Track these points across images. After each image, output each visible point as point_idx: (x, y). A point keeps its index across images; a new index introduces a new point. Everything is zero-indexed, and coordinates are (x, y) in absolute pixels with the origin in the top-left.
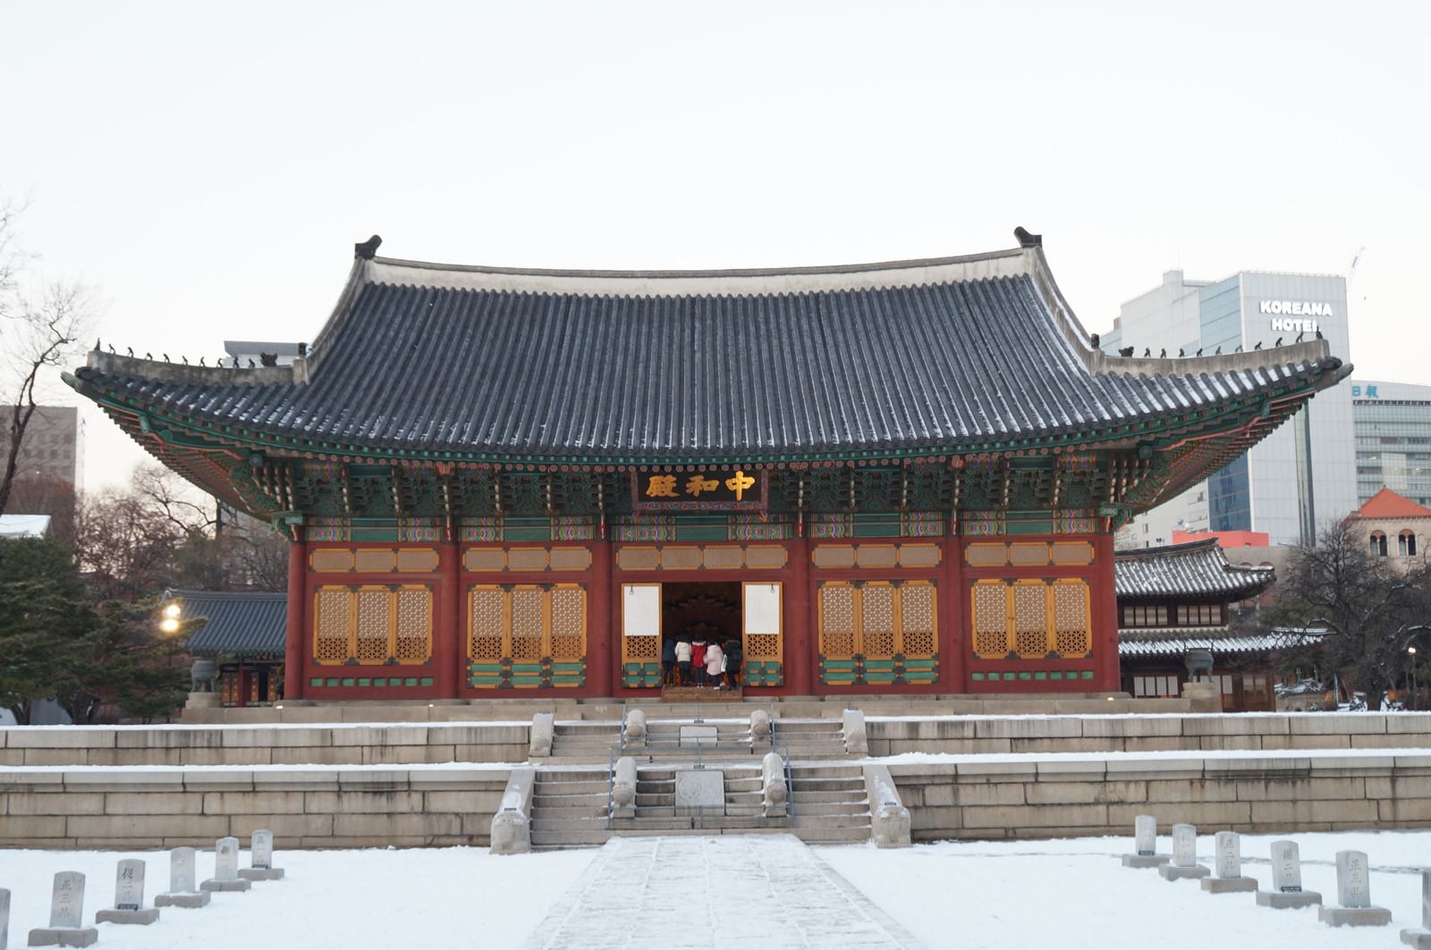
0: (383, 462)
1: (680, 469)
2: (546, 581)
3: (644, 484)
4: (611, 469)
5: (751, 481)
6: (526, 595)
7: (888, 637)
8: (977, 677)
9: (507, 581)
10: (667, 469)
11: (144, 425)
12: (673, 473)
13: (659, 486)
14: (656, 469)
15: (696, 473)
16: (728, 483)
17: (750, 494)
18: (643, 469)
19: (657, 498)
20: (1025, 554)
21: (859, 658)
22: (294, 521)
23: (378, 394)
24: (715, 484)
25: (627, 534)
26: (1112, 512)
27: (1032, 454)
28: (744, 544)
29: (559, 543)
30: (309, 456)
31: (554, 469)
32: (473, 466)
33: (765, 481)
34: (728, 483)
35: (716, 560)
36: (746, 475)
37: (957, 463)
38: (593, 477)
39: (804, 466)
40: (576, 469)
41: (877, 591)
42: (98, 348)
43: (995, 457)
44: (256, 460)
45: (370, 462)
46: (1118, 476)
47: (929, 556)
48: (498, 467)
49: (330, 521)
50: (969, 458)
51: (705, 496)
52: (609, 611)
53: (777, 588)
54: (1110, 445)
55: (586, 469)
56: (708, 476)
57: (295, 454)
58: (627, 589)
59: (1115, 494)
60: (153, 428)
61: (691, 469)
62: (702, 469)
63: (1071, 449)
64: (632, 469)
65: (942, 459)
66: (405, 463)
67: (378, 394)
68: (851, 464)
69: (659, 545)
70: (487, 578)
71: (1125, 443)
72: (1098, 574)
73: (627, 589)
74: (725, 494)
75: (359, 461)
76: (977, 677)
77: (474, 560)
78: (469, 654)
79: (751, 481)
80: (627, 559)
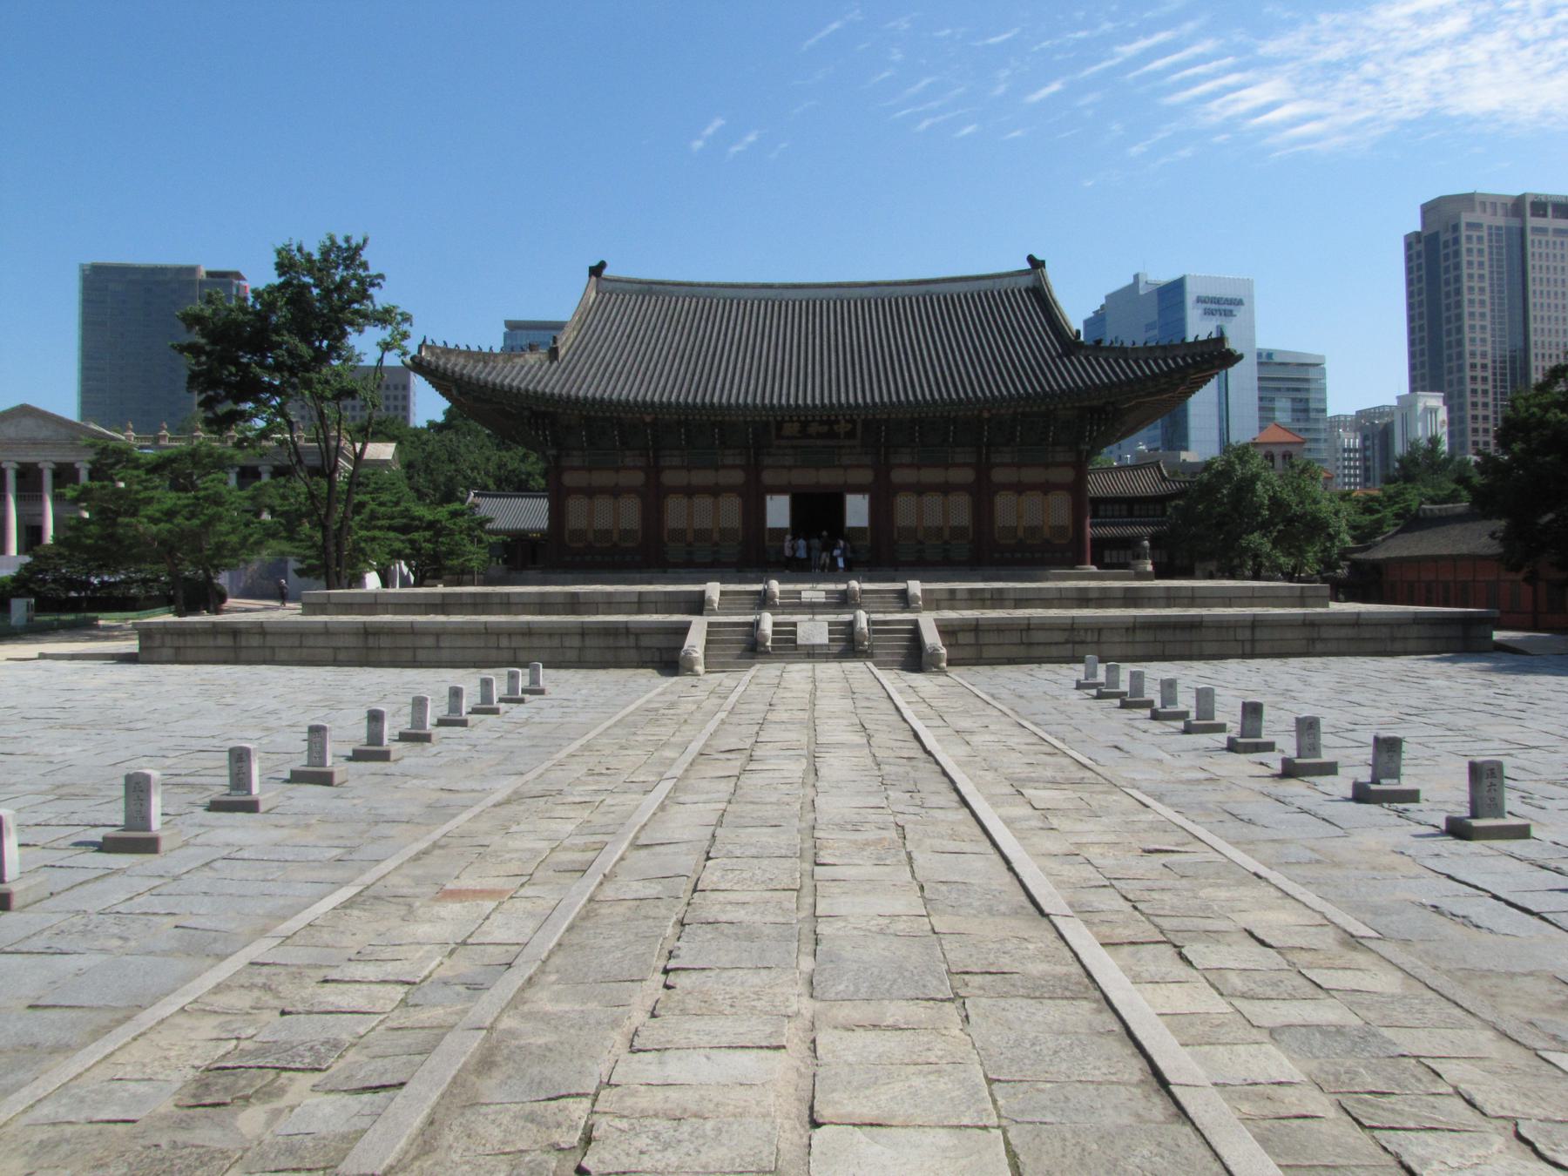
0: (608, 414)
1: (803, 418)
2: (715, 491)
3: (780, 425)
4: (757, 418)
5: (850, 426)
6: (703, 503)
7: (940, 529)
8: (997, 555)
9: (690, 492)
10: (795, 418)
11: (454, 392)
12: (799, 421)
13: (791, 429)
14: (787, 418)
15: (813, 421)
16: (836, 427)
17: (851, 435)
18: (779, 418)
19: (788, 438)
20: (1031, 475)
21: (921, 543)
22: (554, 452)
23: (606, 370)
24: (825, 428)
25: (767, 461)
26: (1088, 447)
27: (1035, 409)
28: (846, 468)
29: (725, 467)
30: (560, 410)
31: (720, 418)
32: (667, 417)
33: (859, 427)
34: (836, 427)
35: (827, 477)
36: (847, 421)
37: (986, 415)
38: (746, 422)
39: (885, 416)
40: (734, 418)
41: (933, 502)
42: (424, 341)
43: (1011, 411)
44: (526, 413)
45: (600, 414)
46: (1092, 427)
47: (965, 475)
48: (683, 418)
49: (575, 453)
50: (994, 411)
51: (820, 436)
52: (755, 512)
53: (867, 497)
54: (1086, 403)
55: (741, 418)
56: (822, 423)
57: (551, 409)
58: (768, 497)
59: (1090, 436)
60: (461, 394)
61: (810, 418)
62: (818, 418)
63: (1060, 406)
64: (771, 418)
65: (976, 412)
66: (622, 415)
67: (606, 370)
68: (916, 415)
69: (790, 468)
70: (675, 490)
71: (1095, 403)
72: (1077, 488)
73: (768, 498)
74: (832, 435)
75: (592, 413)
76: (997, 555)
77: (669, 478)
78: (666, 539)
79: (850, 426)
80: (768, 477)
